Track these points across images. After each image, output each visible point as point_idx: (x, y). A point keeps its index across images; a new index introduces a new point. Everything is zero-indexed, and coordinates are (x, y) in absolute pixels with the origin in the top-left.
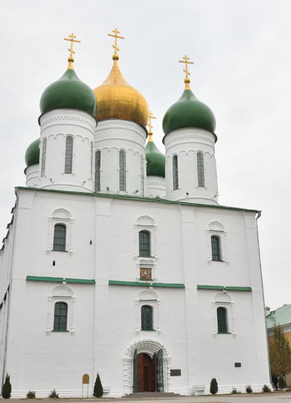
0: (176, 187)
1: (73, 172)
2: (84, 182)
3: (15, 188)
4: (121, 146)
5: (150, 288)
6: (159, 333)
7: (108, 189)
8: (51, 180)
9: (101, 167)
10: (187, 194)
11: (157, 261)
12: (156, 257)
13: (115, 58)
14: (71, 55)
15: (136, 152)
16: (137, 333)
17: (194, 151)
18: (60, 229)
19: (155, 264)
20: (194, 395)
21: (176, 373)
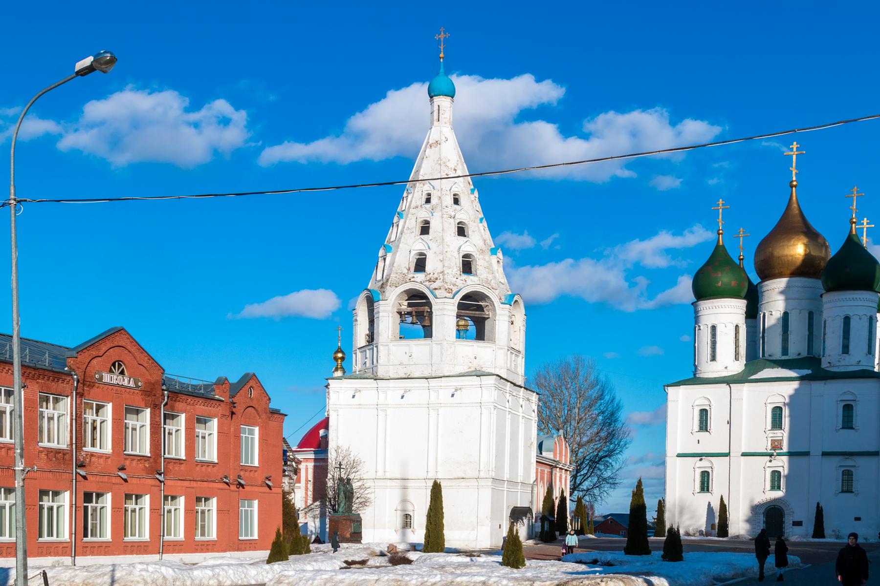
3: (664, 386)
18: (704, 413)
21: (798, 524)
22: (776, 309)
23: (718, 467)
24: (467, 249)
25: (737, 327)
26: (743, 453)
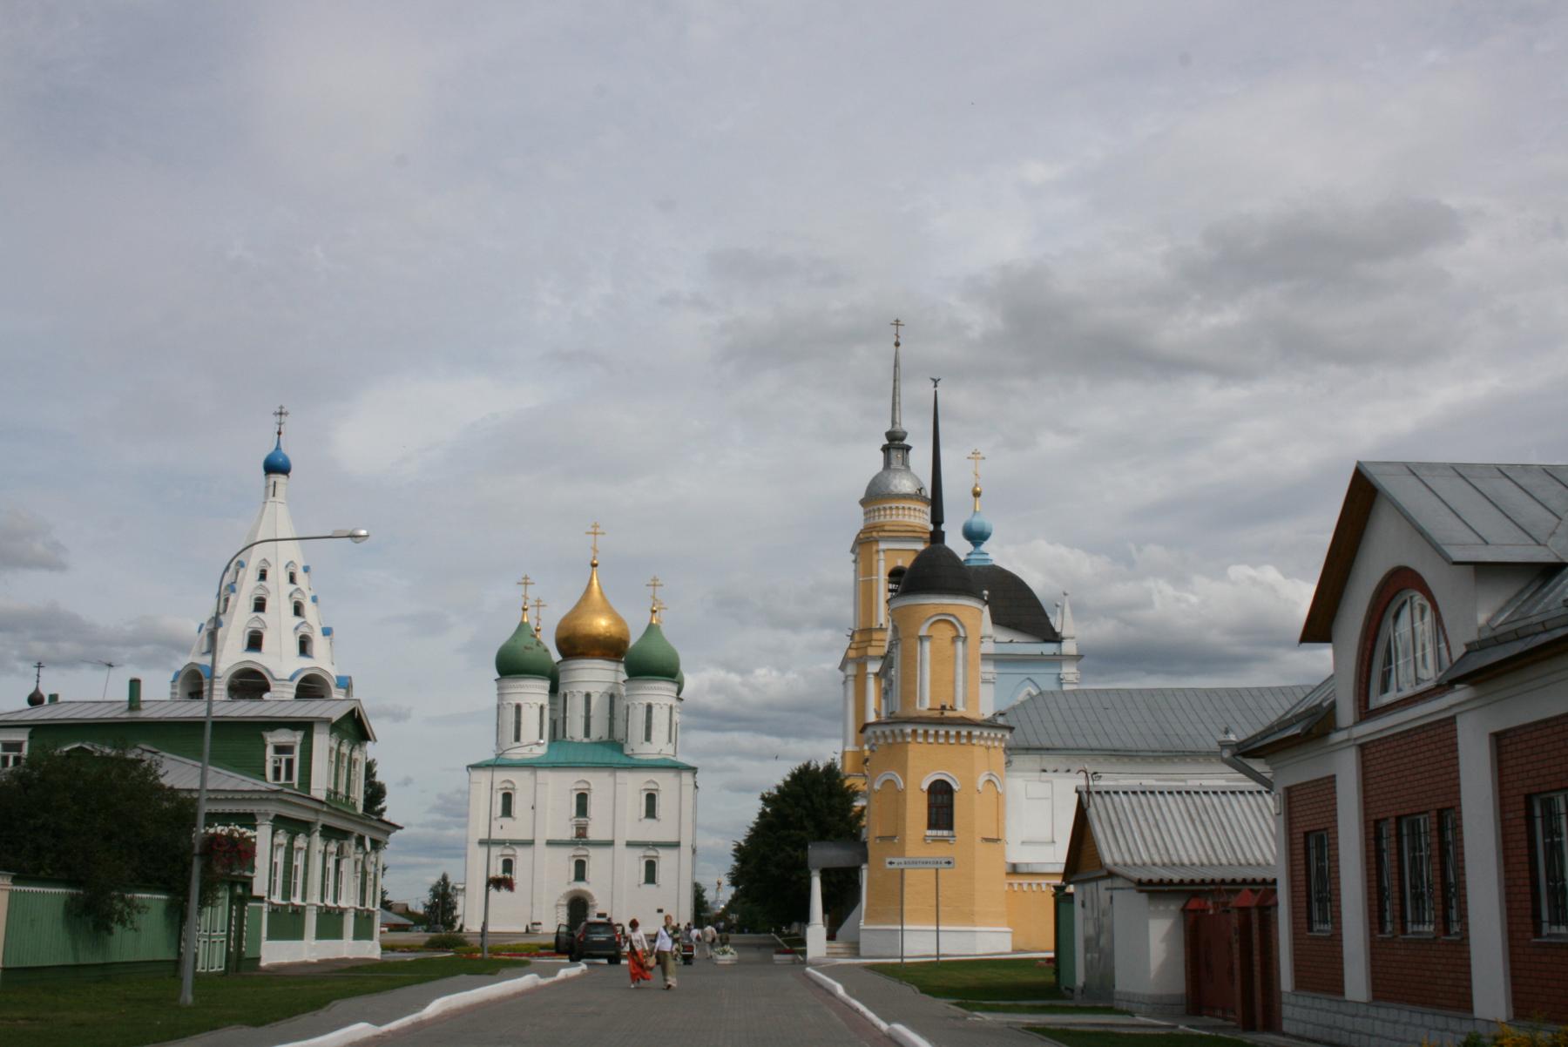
4: (584, 689)
6: (588, 883)
14: (525, 603)
16: (569, 883)
18: (507, 798)
19: (589, 822)
23: (522, 857)
24: (304, 630)
25: (542, 708)
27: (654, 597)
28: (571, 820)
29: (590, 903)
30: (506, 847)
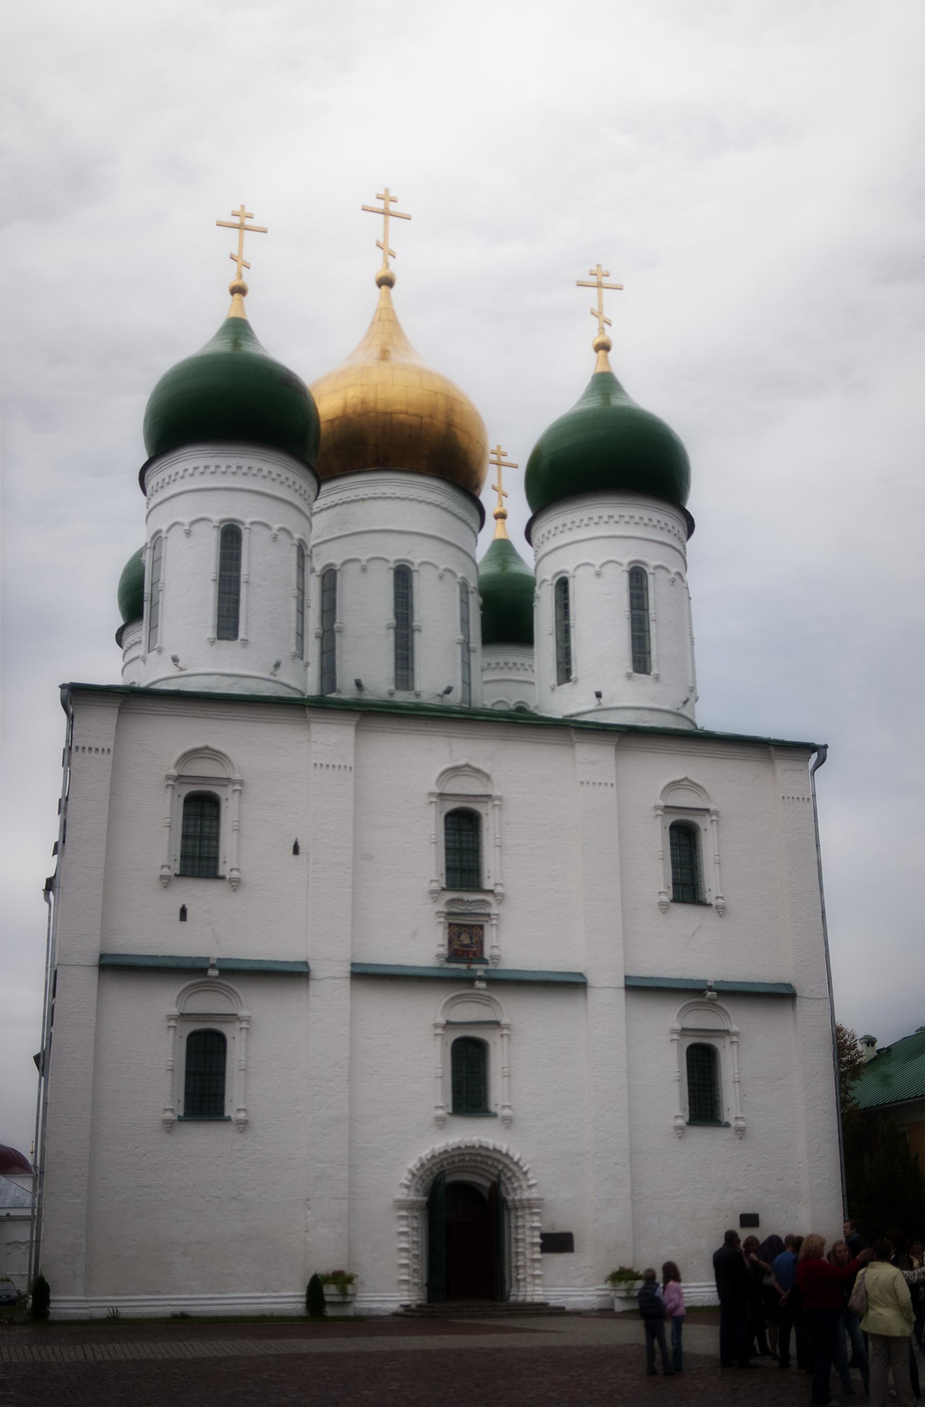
0: (565, 672)
1: (242, 634)
2: (277, 665)
3: (63, 687)
5: (479, 984)
6: (508, 1122)
7: (359, 684)
8: (175, 660)
9: (338, 620)
10: (599, 695)
11: (500, 902)
12: (498, 890)
13: (386, 282)
14: (240, 275)
15: (447, 570)
17: (621, 564)
19: (494, 910)
20: (613, 1310)
22: (370, 556)
26: (353, 965)
27: (598, 314)
28: (434, 895)
29: (513, 1197)
30: (210, 986)
